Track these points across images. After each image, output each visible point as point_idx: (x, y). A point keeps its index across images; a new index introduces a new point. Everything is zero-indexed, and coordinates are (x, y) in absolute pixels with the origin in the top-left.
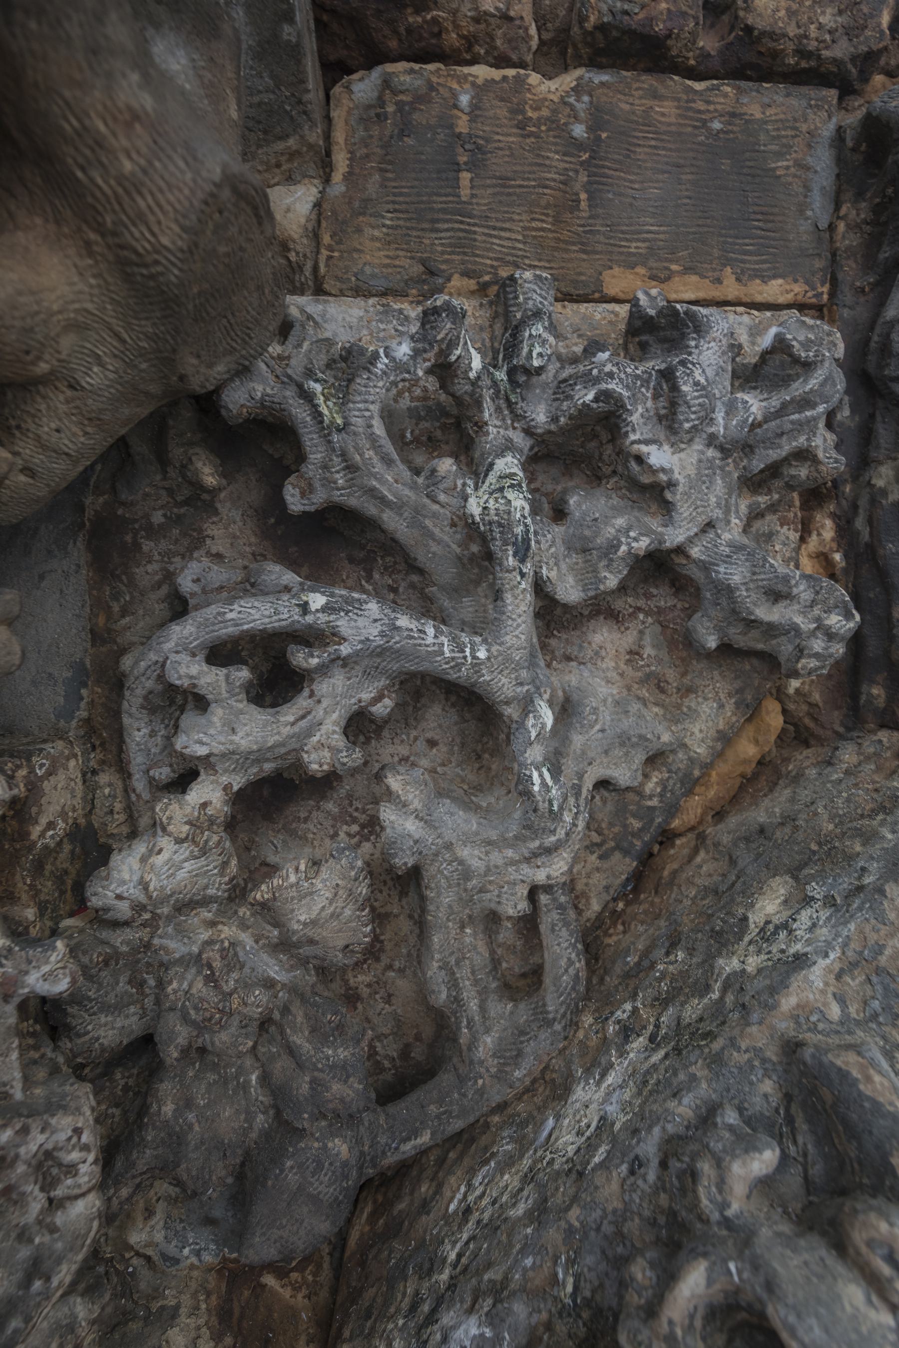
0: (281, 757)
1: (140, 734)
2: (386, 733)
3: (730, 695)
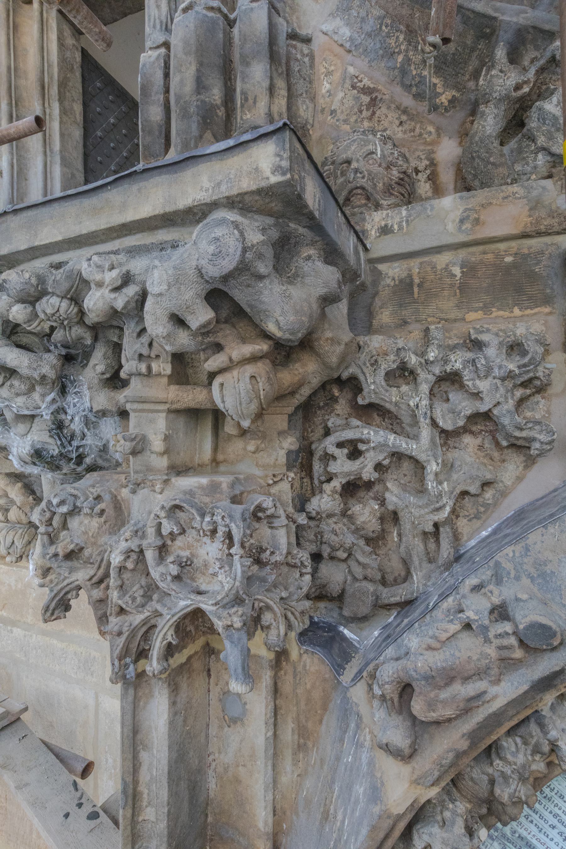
0: (356, 475)
1: (317, 467)
2: (389, 471)
3: (521, 463)
